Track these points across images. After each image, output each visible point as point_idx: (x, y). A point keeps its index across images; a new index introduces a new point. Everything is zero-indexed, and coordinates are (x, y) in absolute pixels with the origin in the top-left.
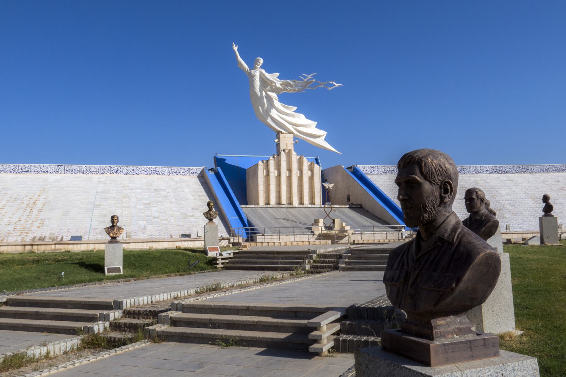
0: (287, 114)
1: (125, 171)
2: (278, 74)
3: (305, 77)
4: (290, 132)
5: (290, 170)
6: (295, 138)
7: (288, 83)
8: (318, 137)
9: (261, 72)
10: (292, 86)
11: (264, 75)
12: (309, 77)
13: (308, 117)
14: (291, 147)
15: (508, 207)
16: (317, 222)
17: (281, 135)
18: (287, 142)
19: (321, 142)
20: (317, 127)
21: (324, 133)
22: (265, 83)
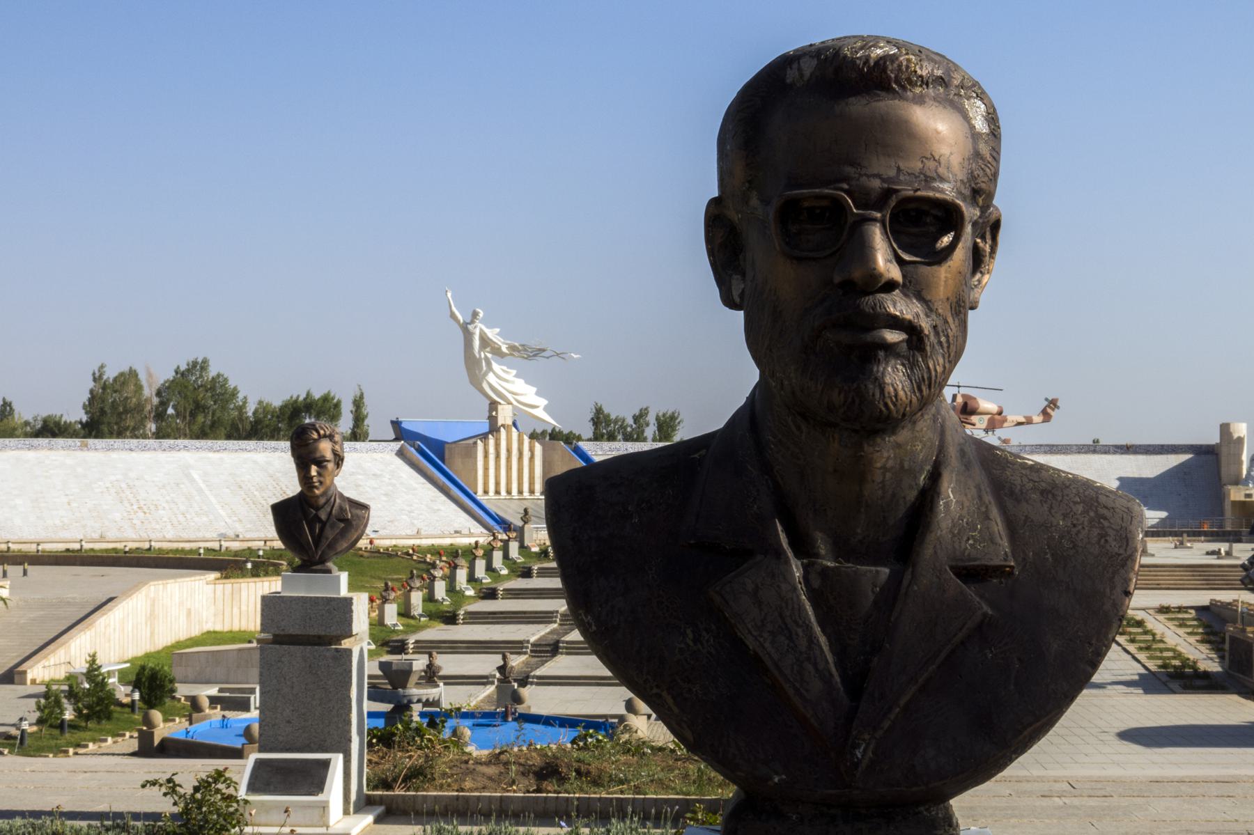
2: (498, 330)
4: (509, 403)
5: (509, 451)
6: (515, 408)
13: (527, 382)
17: (500, 407)
18: (505, 415)
19: (540, 413)
20: (538, 394)
21: (543, 402)
22: (485, 342)
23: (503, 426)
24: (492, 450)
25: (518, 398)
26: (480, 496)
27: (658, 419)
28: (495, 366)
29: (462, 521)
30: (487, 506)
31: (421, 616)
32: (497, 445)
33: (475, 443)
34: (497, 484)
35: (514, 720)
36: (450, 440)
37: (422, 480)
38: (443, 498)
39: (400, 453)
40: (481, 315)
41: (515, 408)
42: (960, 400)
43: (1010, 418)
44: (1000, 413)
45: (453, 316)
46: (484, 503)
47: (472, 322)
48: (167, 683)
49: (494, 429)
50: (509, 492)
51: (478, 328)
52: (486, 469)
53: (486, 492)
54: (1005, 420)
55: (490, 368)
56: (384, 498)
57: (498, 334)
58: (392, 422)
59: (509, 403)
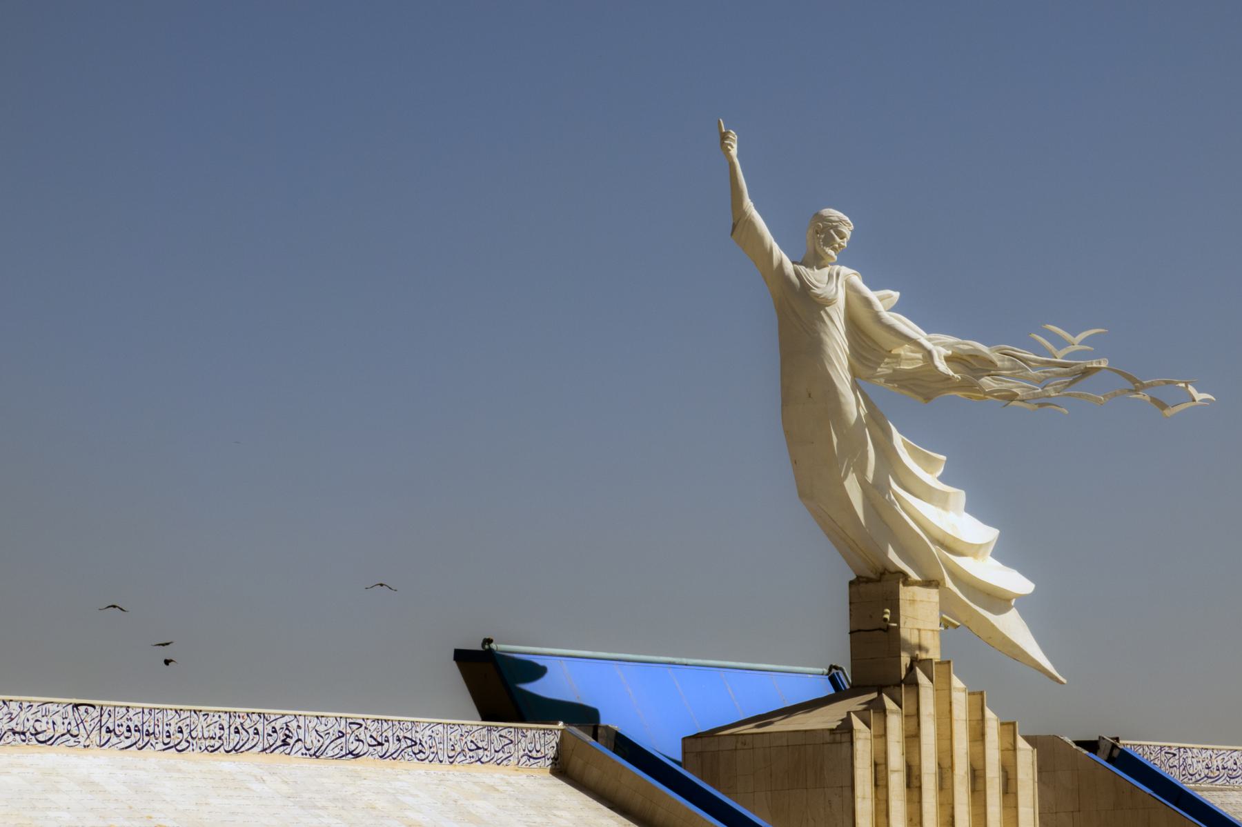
1: (311, 740)
3: (1060, 343)
6: (947, 603)
7: (976, 356)
8: (997, 600)
9: (850, 287)
11: (868, 303)
12: (1077, 341)
17: (905, 593)
19: (1012, 626)
21: (1016, 583)
25: (958, 560)
33: (846, 728)
49: (877, 668)
58: (462, 657)
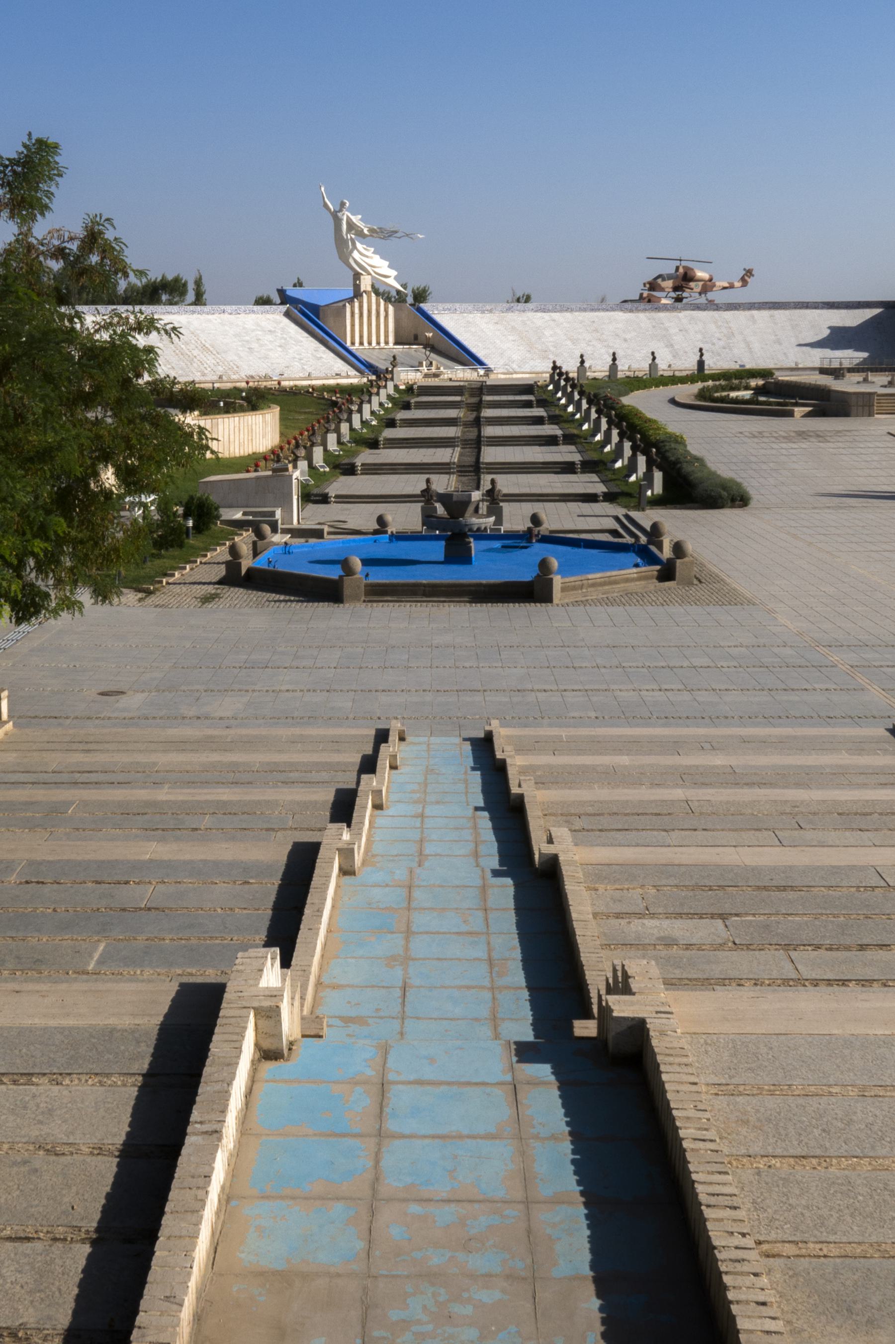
0: (367, 257)
2: (360, 217)
4: (369, 274)
6: (373, 278)
9: (348, 217)
10: (377, 233)
14: (369, 289)
15: (551, 348)
16: (421, 364)
17: (362, 277)
18: (366, 283)
19: (392, 282)
20: (389, 266)
21: (393, 273)
22: (351, 226)
23: (365, 291)
24: (357, 311)
25: (375, 269)
26: (348, 344)
27: (413, 291)
28: (358, 245)
29: (339, 366)
30: (358, 354)
31: (349, 442)
32: (361, 307)
33: (345, 305)
34: (361, 337)
35: (539, 541)
36: (322, 304)
37: (306, 335)
38: (323, 348)
39: (287, 314)
40: (347, 205)
41: (373, 278)
42: (681, 270)
43: (718, 284)
44: (711, 280)
45: (325, 205)
46: (354, 351)
47: (341, 210)
48: (213, 510)
50: (370, 343)
51: (345, 215)
52: (353, 325)
53: (353, 343)
54: (714, 286)
55: (355, 247)
56: (280, 349)
57: (361, 220)
58: (278, 290)
59: (369, 274)
